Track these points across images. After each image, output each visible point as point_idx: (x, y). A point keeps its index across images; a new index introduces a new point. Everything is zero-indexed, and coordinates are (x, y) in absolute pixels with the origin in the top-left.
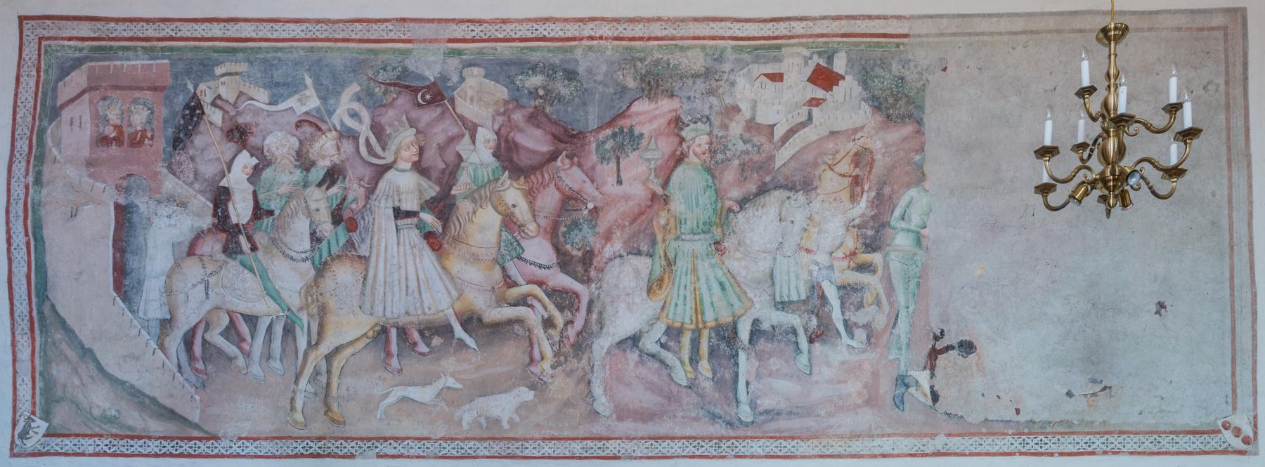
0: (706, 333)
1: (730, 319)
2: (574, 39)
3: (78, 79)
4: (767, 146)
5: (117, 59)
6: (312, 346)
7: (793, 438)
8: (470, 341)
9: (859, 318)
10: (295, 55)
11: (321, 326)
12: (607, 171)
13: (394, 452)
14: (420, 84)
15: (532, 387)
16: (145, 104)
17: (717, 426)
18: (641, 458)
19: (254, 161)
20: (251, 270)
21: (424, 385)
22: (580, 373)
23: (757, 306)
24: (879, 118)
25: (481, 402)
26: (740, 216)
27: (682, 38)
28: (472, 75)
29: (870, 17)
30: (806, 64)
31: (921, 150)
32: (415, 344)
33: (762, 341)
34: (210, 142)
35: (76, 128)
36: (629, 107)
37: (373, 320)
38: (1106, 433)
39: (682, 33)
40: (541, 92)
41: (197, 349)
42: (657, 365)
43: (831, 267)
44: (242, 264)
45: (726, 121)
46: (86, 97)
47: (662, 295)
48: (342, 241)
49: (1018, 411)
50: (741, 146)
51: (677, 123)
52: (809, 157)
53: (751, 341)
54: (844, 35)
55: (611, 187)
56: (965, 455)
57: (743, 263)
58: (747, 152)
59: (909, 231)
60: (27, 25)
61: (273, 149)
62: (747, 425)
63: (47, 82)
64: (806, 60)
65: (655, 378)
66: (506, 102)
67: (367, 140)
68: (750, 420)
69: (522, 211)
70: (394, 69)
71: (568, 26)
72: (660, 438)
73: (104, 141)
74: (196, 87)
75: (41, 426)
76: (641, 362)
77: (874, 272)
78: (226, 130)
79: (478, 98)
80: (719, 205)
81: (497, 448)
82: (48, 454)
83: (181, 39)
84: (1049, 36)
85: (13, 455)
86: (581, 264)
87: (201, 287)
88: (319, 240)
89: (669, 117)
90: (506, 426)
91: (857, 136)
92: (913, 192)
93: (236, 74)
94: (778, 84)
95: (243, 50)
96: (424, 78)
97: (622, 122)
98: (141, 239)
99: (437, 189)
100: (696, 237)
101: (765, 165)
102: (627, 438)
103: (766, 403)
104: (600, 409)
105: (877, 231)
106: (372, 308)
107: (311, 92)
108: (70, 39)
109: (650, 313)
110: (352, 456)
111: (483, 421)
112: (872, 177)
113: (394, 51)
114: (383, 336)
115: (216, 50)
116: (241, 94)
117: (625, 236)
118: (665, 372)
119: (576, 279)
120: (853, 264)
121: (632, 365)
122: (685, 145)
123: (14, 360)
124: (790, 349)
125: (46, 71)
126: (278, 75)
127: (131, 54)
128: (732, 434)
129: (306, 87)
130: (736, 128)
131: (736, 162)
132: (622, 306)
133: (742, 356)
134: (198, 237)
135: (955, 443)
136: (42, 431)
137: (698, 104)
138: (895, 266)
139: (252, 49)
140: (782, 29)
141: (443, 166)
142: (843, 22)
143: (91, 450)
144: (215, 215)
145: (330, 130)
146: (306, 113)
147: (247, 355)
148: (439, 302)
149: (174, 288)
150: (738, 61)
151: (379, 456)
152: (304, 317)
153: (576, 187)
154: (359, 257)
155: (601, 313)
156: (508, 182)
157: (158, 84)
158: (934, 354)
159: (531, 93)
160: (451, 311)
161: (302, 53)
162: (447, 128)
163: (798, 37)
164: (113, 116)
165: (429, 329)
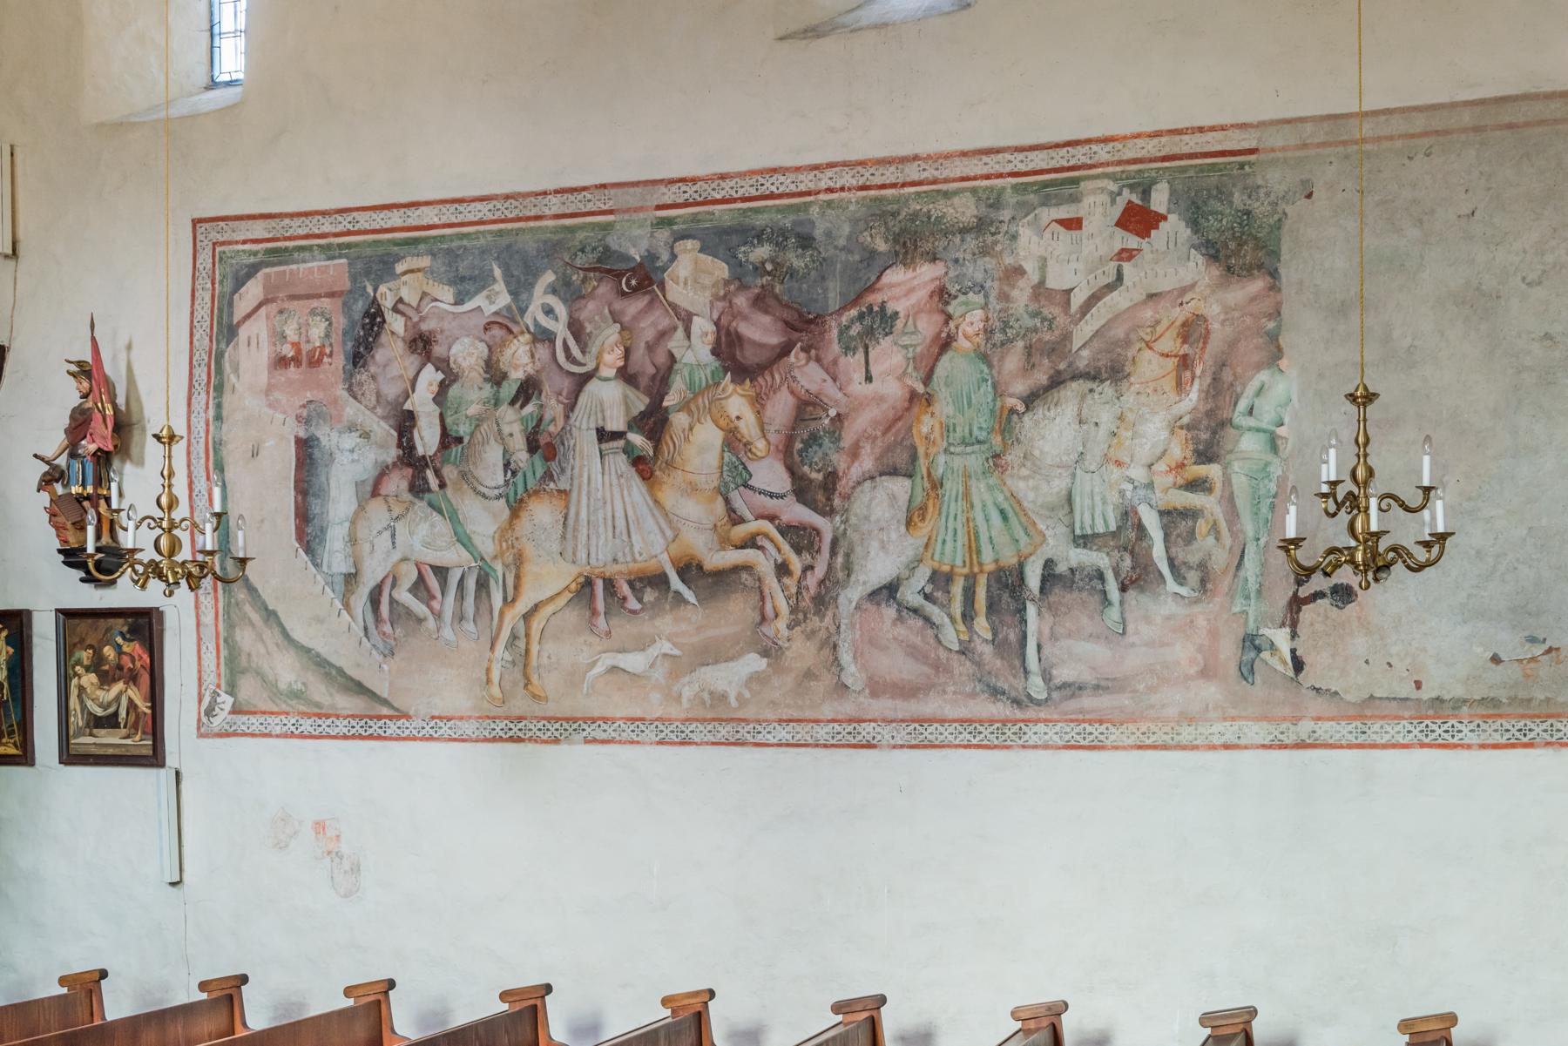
0: (982, 581)
1: (1014, 561)
2: (809, 193)
3: (253, 290)
5: (293, 262)
6: (508, 602)
7: (1101, 722)
8: (689, 595)
10: (482, 241)
11: (518, 577)
13: (604, 736)
14: (623, 266)
15: (765, 653)
16: (322, 314)
17: (999, 705)
18: (902, 746)
19: (440, 376)
20: (440, 512)
22: (823, 634)
23: (1051, 541)
24: (1216, 271)
26: (1026, 418)
27: (946, 181)
28: (685, 251)
29: (1201, 130)
30: (1113, 202)
31: (1276, 313)
32: (625, 599)
34: (392, 354)
36: (879, 278)
37: (575, 570)
38: (1550, 716)
39: (945, 174)
40: (769, 267)
42: (920, 623)
43: (1150, 486)
44: (430, 505)
45: (1006, 288)
46: (263, 310)
47: (925, 529)
48: (540, 472)
49: (1418, 685)
51: (942, 295)
52: (1119, 332)
53: (1042, 590)
54: (1164, 159)
56: (1341, 747)
57: (1031, 483)
58: (1035, 330)
59: (1258, 430)
60: (201, 228)
61: (460, 360)
62: (1038, 703)
63: (222, 295)
64: (1114, 196)
65: (918, 640)
66: (727, 283)
68: (1043, 696)
69: (748, 425)
70: (594, 249)
71: (801, 177)
72: (925, 721)
73: (281, 362)
74: (375, 290)
75: (226, 701)
76: (900, 619)
78: (408, 338)
79: (693, 279)
80: (999, 404)
81: (723, 732)
82: (235, 734)
83: (359, 232)
84: (1463, 137)
85: (201, 736)
86: (820, 490)
87: (387, 534)
88: (514, 473)
89: (932, 287)
90: (734, 703)
91: (1187, 298)
92: (1263, 376)
94: (1074, 233)
95: (425, 240)
96: (626, 258)
98: (323, 479)
100: (969, 449)
101: (1059, 347)
102: (884, 720)
103: (1063, 674)
104: (849, 682)
105: (1214, 433)
106: (574, 554)
107: (500, 286)
108: (244, 242)
109: (910, 553)
110: (556, 741)
111: (706, 696)
112: (1206, 357)
113: (593, 226)
114: (587, 590)
115: (396, 243)
116: (424, 295)
117: (878, 450)
118: (930, 632)
119: (815, 510)
120: (1180, 481)
121: (888, 623)
122: (952, 324)
123: (198, 625)
125: (221, 282)
126: (463, 267)
127: (307, 255)
128: (1019, 715)
131: (1020, 344)
132: (875, 544)
133: (1031, 610)
135: (1326, 730)
136: (228, 707)
137: (969, 269)
138: (1240, 482)
140: (1079, 155)
142: (1164, 140)
143: (278, 730)
144: (400, 445)
146: (496, 313)
147: (438, 616)
149: (359, 535)
151: (587, 741)
152: (499, 568)
153: (814, 388)
154: (559, 491)
155: (847, 555)
156: (731, 387)
157: (335, 289)
158: (1296, 603)
159: (756, 269)
160: (665, 557)
161: (489, 238)
163: (1102, 165)
164: (291, 332)
165: (641, 579)
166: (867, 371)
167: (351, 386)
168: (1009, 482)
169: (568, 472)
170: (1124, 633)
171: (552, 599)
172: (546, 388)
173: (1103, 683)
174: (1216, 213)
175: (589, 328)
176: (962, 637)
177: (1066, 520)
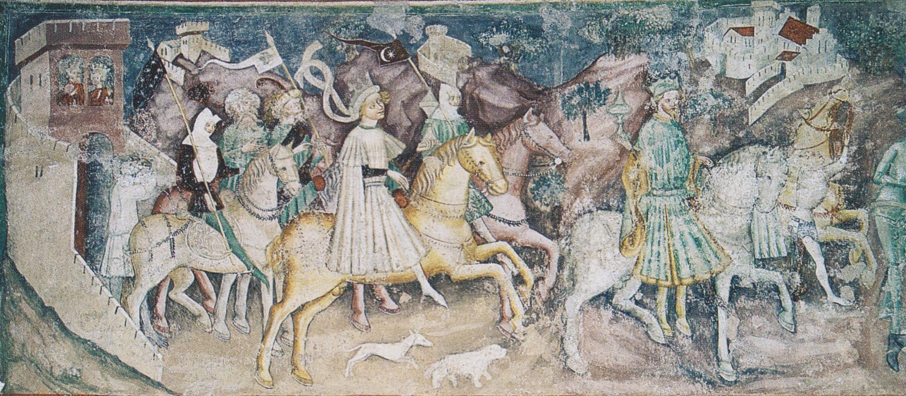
0: (682, 290)
1: (708, 276)
3: (36, 37)
4: (739, 101)
5: (79, 17)
9: (845, 275)
10: (256, 13)
11: (286, 283)
12: (574, 127)
15: (504, 345)
16: (105, 63)
17: (698, 385)
19: (217, 119)
21: (393, 342)
23: (735, 261)
24: (856, 71)
25: (452, 361)
26: (713, 171)
30: (777, 18)
32: (382, 301)
33: (743, 297)
35: (36, 87)
36: (594, 63)
37: (339, 278)
40: (506, 49)
41: (161, 307)
42: (632, 322)
43: (812, 224)
44: (208, 222)
45: (695, 76)
47: (635, 251)
48: (310, 199)
50: (711, 101)
51: (645, 79)
53: (730, 299)
55: (578, 142)
61: (235, 106)
62: (730, 384)
64: (778, 13)
65: (631, 336)
66: (471, 60)
67: (331, 99)
68: (733, 379)
69: (490, 169)
74: (156, 46)
76: (616, 319)
77: (859, 228)
87: (167, 245)
88: (287, 199)
90: (478, 385)
91: (835, 88)
93: (198, 33)
97: (587, 78)
99: (404, 146)
100: (668, 193)
101: (737, 121)
103: (747, 362)
105: (860, 187)
107: (273, 50)
116: (204, 52)
117: (595, 191)
119: (545, 234)
120: (835, 221)
121: (606, 323)
124: (772, 308)
126: (239, 32)
127: (90, 12)
129: (268, 46)
130: (706, 84)
131: (707, 117)
133: (721, 313)
134: (164, 194)
137: (666, 59)
138: (882, 221)
139: (214, 8)
141: (410, 124)
144: (179, 173)
145: (293, 88)
146: (269, 72)
147: (213, 313)
148: (407, 261)
150: (706, 15)
153: (543, 143)
155: (572, 270)
156: (475, 139)
159: (495, 50)
162: (409, 85)
164: (73, 73)
165: (397, 286)
166: (585, 132)
167: (132, 122)
168: (702, 218)
169: (335, 199)
170: (795, 332)
171: (317, 300)
172: (315, 133)
173: (779, 369)
174: (856, 29)
175: (352, 87)
176: (666, 333)
177: (748, 248)
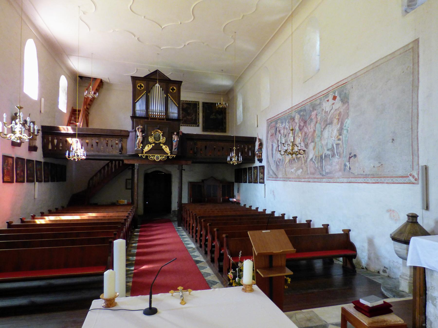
103: (327, 171)
158: (350, 158)
